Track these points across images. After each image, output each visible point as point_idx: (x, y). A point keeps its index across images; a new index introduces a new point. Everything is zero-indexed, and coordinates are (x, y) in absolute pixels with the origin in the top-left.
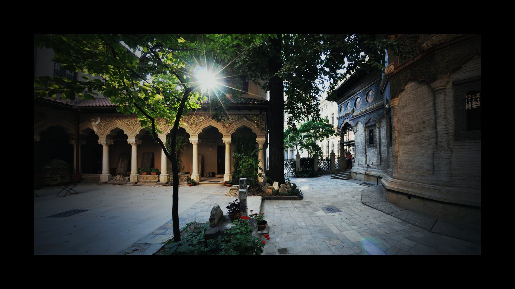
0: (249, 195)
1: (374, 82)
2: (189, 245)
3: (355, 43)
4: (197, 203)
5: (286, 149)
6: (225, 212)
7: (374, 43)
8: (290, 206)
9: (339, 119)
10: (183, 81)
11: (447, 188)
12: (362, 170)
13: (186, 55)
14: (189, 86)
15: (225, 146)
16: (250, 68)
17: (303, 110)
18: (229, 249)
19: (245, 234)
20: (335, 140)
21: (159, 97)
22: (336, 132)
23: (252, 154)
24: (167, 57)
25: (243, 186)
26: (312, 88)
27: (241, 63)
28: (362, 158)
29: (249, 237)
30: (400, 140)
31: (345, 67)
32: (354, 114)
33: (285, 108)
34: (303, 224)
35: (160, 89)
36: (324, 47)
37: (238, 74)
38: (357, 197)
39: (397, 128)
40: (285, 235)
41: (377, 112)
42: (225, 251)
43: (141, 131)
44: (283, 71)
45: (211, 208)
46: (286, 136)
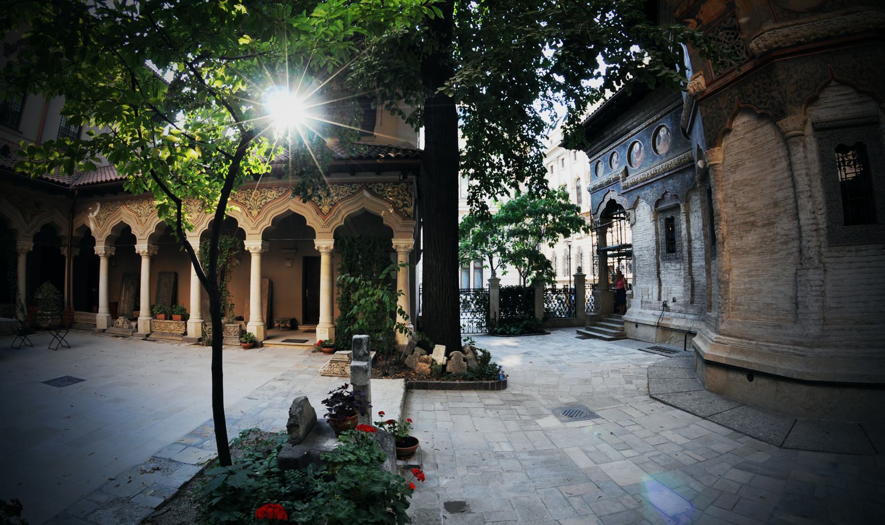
0: (375, 376)
1: (667, 109)
2: (250, 476)
3: (618, 27)
4: (261, 388)
6: (322, 412)
7: (657, 31)
8: (474, 405)
9: (593, 191)
10: (238, 117)
11: (817, 350)
12: (650, 317)
13: (249, 67)
14: (250, 127)
15: (319, 258)
16: (380, 79)
17: (506, 170)
18: (333, 493)
19: (367, 465)
20: (583, 243)
21: (194, 154)
22: (588, 222)
23: (382, 277)
24: (215, 75)
26: (526, 118)
27: (361, 70)
28: (650, 286)
29: (376, 473)
30: (732, 243)
31: (599, 74)
32: (629, 180)
33: (463, 167)
34: (506, 448)
35: (197, 138)
36: (550, 32)
37: (354, 93)
38: (639, 382)
39: (723, 215)
40: (462, 471)
41: (680, 176)
42: (323, 497)
43: (159, 227)
44: (456, 82)
45: (291, 402)
46: (465, 233)
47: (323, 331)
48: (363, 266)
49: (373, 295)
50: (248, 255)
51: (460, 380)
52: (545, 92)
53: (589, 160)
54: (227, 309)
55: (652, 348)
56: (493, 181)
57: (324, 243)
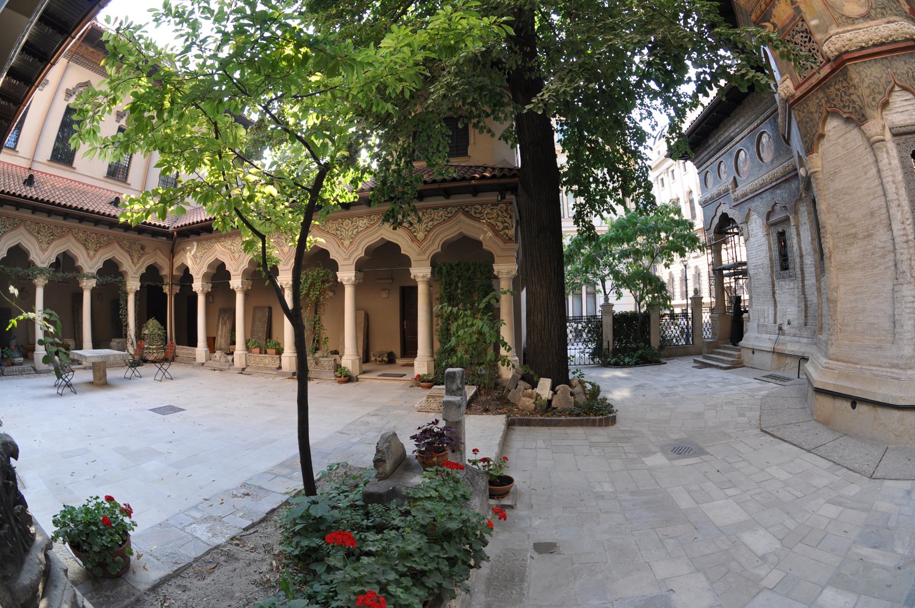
4: (353, 423)
5: (577, 291)
9: (704, 204)
22: (702, 238)
25: (454, 387)
28: (766, 308)
32: (739, 191)
43: (251, 262)
47: (422, 365)
48: (462, 295)
49: (472, 325)
50: (340, 287)
51: (565, 415)
52: (642, 100)
53: (697, 171)
54: (322, 343)
55: (767, 377)
56: (598, 197)
57: (420, 272)
